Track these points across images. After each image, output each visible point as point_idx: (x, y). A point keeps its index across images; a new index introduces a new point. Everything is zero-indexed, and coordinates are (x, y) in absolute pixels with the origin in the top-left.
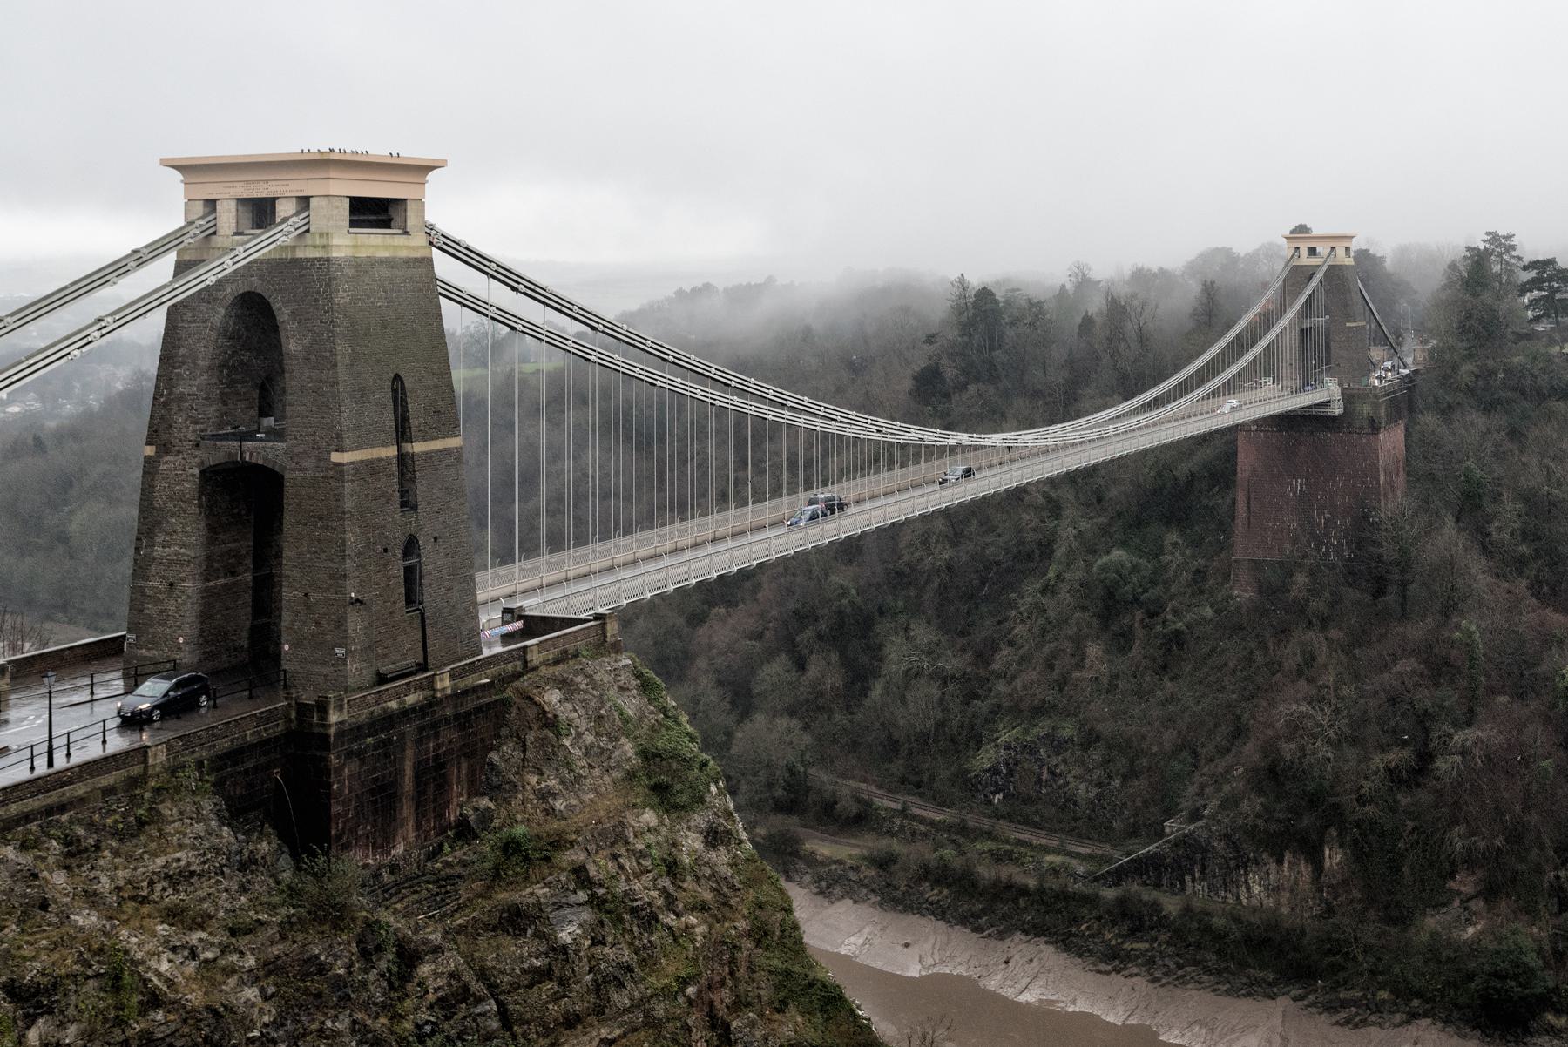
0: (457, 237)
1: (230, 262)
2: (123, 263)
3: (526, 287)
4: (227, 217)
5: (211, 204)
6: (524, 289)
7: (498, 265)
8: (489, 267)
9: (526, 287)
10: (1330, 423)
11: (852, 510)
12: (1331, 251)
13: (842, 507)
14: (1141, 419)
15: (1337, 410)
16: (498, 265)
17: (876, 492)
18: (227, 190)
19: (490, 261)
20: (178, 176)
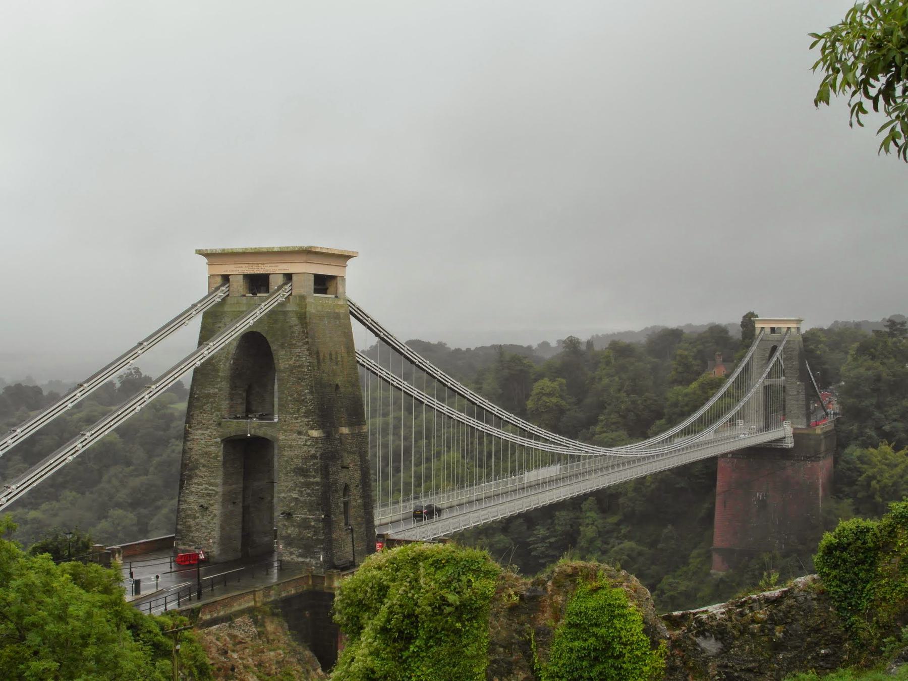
0: (353, 301)
1: (258, 312)
2: (190, 313)
3: (384, 334)
4: (238, 285)
5: (226, 278)
6: (383, 336)
7: (372, 320)
8: (367, 320)
9: (384, 334)
10: (785, 453)
11: (444, 516)
12: (787, 331)
13: (439, 511)
14: (666, 448)
15: (790, 444)
16: (372, 320)
17: (471, 499)
18: (240, 269)
19: (368, 317)
20: (204, 260)
